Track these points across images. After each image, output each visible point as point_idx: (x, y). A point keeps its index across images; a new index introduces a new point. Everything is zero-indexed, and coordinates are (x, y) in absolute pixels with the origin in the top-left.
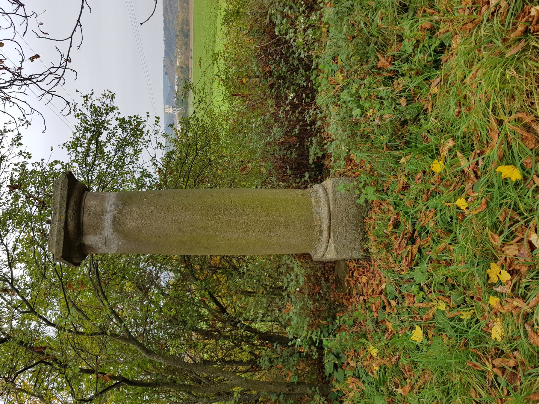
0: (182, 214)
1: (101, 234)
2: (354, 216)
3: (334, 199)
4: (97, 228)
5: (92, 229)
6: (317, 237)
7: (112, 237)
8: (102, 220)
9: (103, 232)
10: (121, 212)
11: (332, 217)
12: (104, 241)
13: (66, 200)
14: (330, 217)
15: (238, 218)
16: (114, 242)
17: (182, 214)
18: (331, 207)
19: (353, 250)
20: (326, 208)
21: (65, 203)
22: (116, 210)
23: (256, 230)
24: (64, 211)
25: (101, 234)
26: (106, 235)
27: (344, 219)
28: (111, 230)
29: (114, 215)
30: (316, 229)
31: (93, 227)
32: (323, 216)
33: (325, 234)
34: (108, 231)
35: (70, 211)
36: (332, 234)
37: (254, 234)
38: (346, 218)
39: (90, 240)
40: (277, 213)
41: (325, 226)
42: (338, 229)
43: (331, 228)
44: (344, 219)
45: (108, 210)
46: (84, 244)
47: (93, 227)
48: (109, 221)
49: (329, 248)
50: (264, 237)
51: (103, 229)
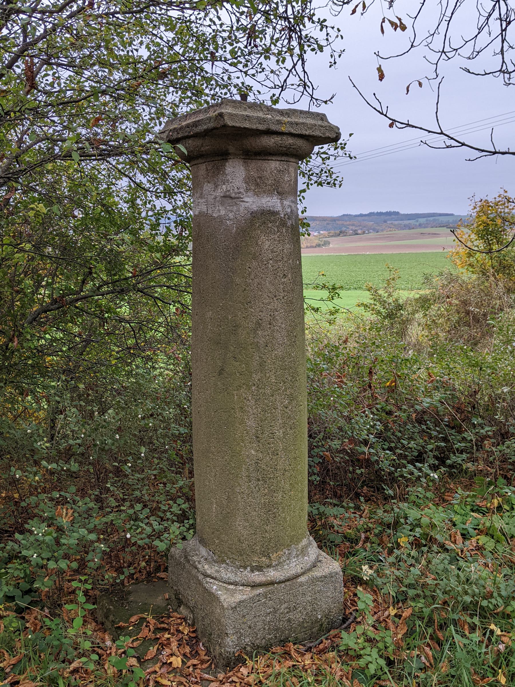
0: (283, 326)
1: (247, 190)
2: (289, 620)
3: (314, 581)
4: (257, 185)
5: (256, 175)
6: (248, 563)
7: (242, 209)
8: (270, 193)
9: (250, 194)
10: (283, 224)
11: (288, 583)
12: (233, 195)
13: (307, 133)
14: (288, 580)
15: (280, 421)
16: (232, 211)
17: (283, 326)
18: (302, 579)
19: (239, 635)
20: (299, 571)
21: (304, 132)
22: (285, 215)
23: (260, 455)
24: (292, 131)
25: (247, 190)
26: (246, 199)
27: (286, 605)
28: (254, 208)
29: (278, 213)
30: (264, 559)
31: (260, 178)
32: (286, 567)
33: (257, 577)
34: (252, 202)
35: (290, 141)
36: (261, 590)
37: (253, 452)
38: (287, 608)
39: (236, 172)
40: (287, 487)
41: (272, 574)
42: (271, 600)
43: (271, 588)
44: (286, 605)
45: (285, 202)
46: (226, 160)
47: (260, 178)
48: (270, 204)
49: (231, 587)
50: (248, 470)
51: (256, 194)
